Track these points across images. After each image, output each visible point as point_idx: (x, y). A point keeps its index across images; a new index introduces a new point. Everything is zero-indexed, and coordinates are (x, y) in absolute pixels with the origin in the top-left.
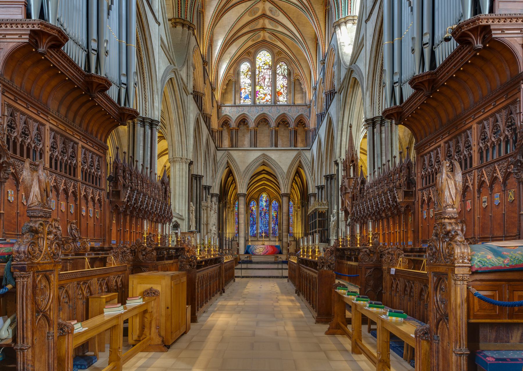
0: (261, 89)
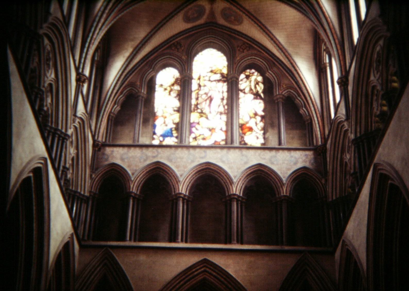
0: (203, 120)
